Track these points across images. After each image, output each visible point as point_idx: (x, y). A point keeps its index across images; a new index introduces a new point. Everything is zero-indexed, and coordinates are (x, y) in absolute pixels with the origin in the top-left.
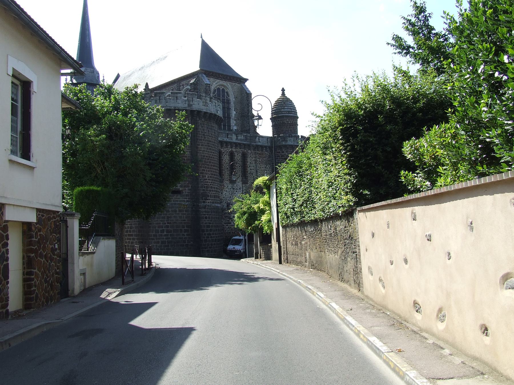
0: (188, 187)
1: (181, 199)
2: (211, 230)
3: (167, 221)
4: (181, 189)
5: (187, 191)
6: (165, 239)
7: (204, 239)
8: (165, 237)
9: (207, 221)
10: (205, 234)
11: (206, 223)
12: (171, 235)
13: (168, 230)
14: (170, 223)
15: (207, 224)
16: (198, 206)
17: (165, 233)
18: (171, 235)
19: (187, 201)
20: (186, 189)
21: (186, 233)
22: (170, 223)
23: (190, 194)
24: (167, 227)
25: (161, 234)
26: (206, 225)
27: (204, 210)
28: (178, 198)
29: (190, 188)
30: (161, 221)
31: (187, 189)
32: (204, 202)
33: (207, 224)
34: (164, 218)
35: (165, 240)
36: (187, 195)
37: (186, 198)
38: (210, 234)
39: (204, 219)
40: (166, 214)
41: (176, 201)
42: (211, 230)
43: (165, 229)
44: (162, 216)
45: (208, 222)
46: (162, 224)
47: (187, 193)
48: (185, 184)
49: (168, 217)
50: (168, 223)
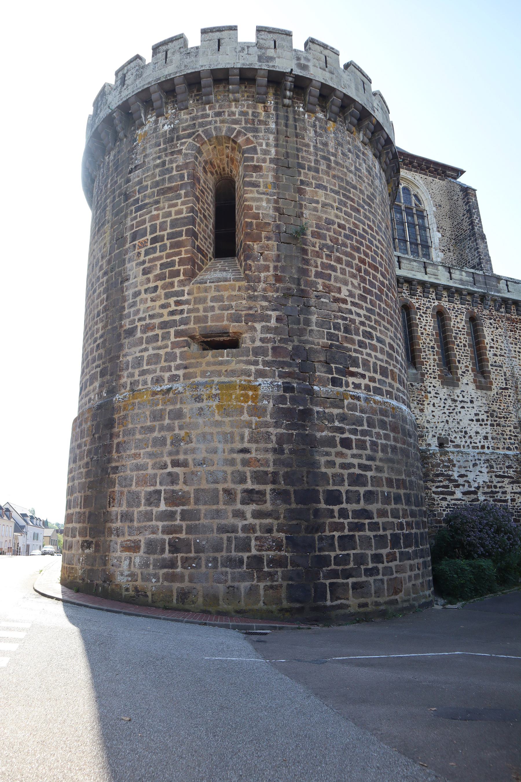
0: (267, 318)
1: (233, 366)
2: (370, 496)
3: (170, 454)
4: (233, 327)
5: (259, 335)
6: (163, 532)
7: (337, 534)
8: (160, 524)
9: (354, 456)
10: (343, 513)
11: (343, 466)
12: (184, 515)
13: (173, 491)
14: (185, 464)
15: (352, 471)
16: (311, 392)
17: (163, 507)
18: (184, 515)
19: (260, 374)
20: (254, 329)
21: (254, 507)
22: (185, 464)
23: (274, 348)
24: (173, 478)
25: (149, 508)
26: (345, 472)
27: (336, 411)
28: (221, 363)
29: (273, 323)
30: (151, 455)
31: (258, 326)
32: (335, 382)
33: (352, 471)
34: (162, 442)
35: (160, 536)
36: (257, 352)
37: (256, 363)
38: (365, 514)
39: (335, 446)
40: (170, 428)
41: (213, 373)
42: (370, 496)
43: (162, 488)
44: (156, 434)
45: (356, 461)
46: (154, 467)
47: (258, 344)
48: (250, 308)
49: (176, 441)
50: (176, 464)
